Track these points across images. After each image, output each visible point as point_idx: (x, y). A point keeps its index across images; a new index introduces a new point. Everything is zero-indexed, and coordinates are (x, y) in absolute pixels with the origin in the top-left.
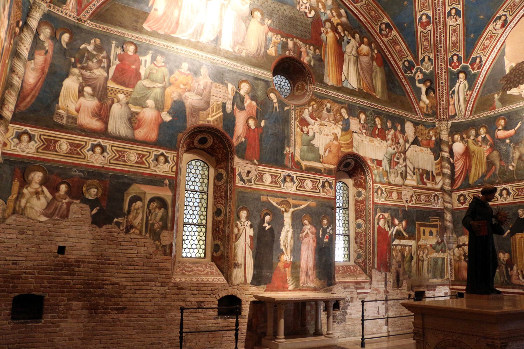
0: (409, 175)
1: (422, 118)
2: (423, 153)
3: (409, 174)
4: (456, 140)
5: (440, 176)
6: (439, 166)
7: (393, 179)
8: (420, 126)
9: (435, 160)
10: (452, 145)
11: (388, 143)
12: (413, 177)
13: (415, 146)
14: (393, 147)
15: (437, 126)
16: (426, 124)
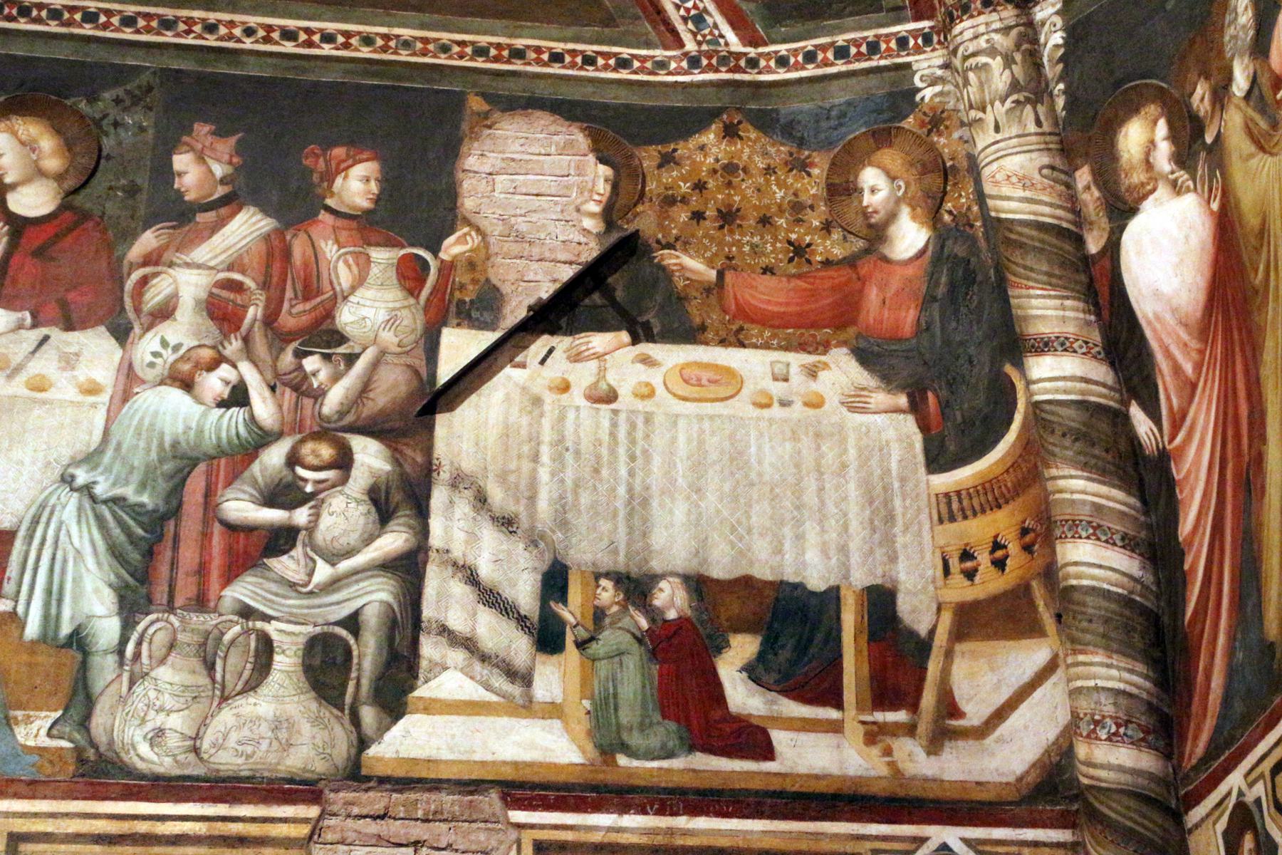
0: (457, 656)
1: (729, 60)
2: (741, 407)
3: (468, 644)
4: (1138, 177)
5: (1033, 630)
6: (1002, 522)
7: (175, 722)
8: (710, 137)
9: (937, 460)
10: (1113, 248)
11: (147, 346)
12: (524, 678)
13: (599, 341)
14: (215, 383)
15: (928, 93)
16: (799, 106)
